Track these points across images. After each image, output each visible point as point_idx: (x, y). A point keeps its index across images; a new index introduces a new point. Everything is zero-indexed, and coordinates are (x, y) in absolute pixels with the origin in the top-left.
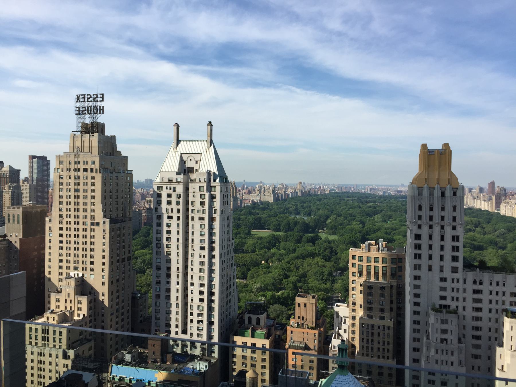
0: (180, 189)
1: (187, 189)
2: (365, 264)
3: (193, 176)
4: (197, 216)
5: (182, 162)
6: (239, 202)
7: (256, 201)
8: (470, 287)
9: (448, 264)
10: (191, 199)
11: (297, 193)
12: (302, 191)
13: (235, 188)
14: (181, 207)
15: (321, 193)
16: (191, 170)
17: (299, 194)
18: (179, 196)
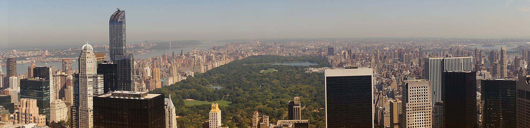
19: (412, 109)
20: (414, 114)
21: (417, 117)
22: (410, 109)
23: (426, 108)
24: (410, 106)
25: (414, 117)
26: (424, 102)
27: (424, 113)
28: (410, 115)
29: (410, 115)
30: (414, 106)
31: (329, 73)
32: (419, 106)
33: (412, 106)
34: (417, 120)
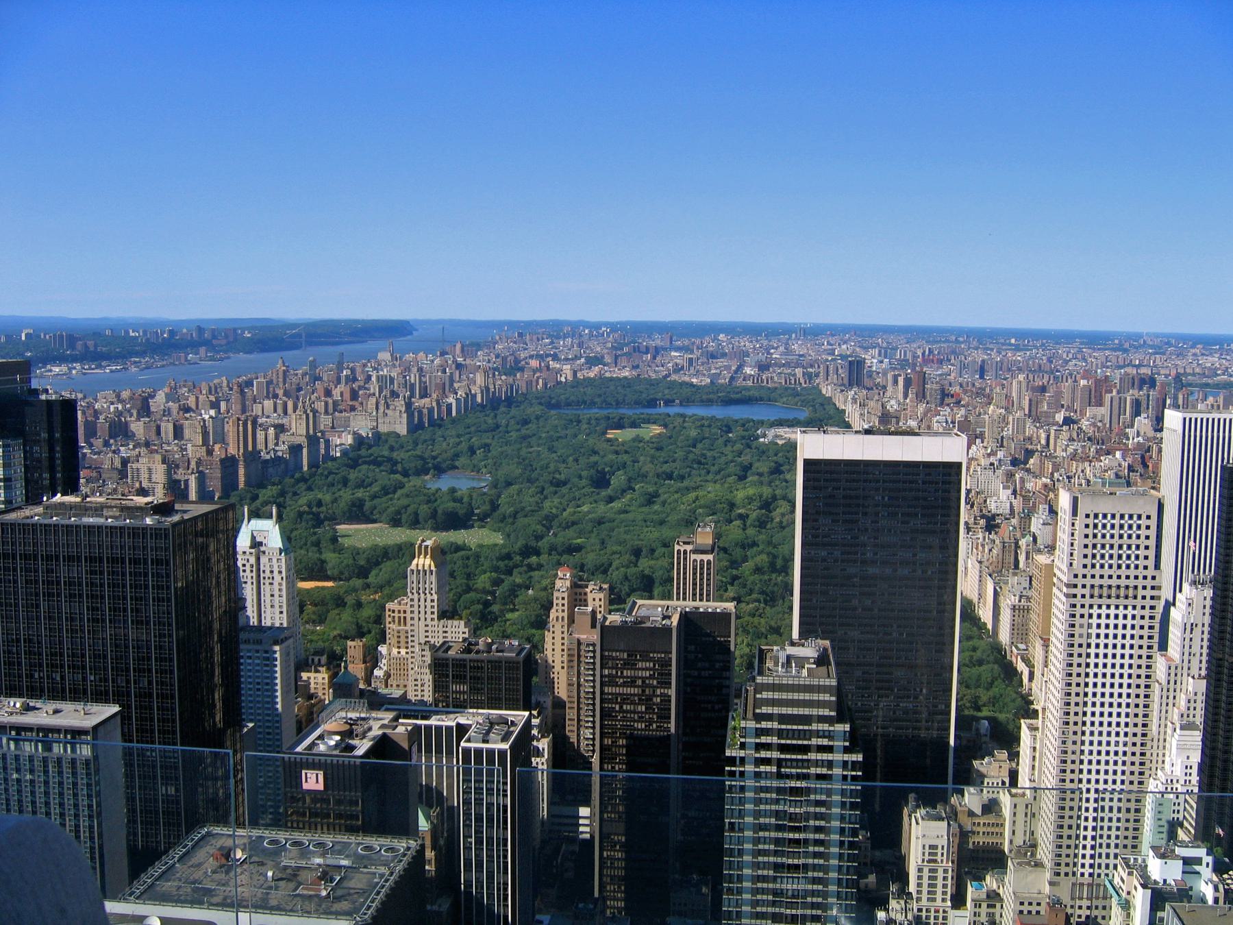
0: (253, 560)
1: (258, 559)
2: (396, 615)
3: (262, 549)
4: (267, 582)
5: (253, 538)
6: (322, 446)
7: (364, 435)
8: (441, 629)
9: (429, 616)
10: (262, 568)
11: (474, 396)
12: (487, 389)
13: (311, 415)
14: (254, 574)
15: (545, 384)
16: (261, 544)
17: (479, 400)
18: (252, 566)
19: (1087, 591)
20: (1095, 611)
21: (1103, 621)
22: (1079, 591)
23: (1140, 593)
24: (1080, 581)
25: (1094, 621)
26: (1132, 572)
27: (1130, 612)
28: (1079, 611)
29: (1079, 611)
30: (1097, 582)
31: (815, 445)
32: (1114, 582)
33: (1088, 581)
34: (1103, 631)
